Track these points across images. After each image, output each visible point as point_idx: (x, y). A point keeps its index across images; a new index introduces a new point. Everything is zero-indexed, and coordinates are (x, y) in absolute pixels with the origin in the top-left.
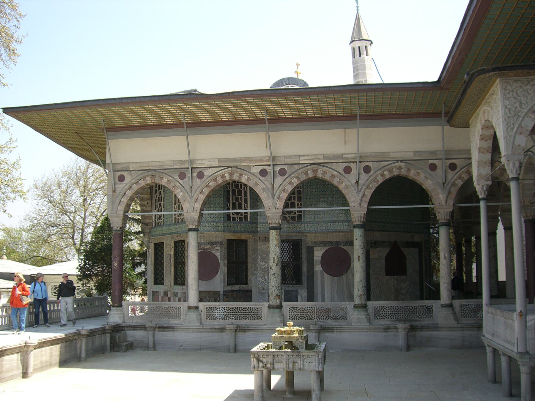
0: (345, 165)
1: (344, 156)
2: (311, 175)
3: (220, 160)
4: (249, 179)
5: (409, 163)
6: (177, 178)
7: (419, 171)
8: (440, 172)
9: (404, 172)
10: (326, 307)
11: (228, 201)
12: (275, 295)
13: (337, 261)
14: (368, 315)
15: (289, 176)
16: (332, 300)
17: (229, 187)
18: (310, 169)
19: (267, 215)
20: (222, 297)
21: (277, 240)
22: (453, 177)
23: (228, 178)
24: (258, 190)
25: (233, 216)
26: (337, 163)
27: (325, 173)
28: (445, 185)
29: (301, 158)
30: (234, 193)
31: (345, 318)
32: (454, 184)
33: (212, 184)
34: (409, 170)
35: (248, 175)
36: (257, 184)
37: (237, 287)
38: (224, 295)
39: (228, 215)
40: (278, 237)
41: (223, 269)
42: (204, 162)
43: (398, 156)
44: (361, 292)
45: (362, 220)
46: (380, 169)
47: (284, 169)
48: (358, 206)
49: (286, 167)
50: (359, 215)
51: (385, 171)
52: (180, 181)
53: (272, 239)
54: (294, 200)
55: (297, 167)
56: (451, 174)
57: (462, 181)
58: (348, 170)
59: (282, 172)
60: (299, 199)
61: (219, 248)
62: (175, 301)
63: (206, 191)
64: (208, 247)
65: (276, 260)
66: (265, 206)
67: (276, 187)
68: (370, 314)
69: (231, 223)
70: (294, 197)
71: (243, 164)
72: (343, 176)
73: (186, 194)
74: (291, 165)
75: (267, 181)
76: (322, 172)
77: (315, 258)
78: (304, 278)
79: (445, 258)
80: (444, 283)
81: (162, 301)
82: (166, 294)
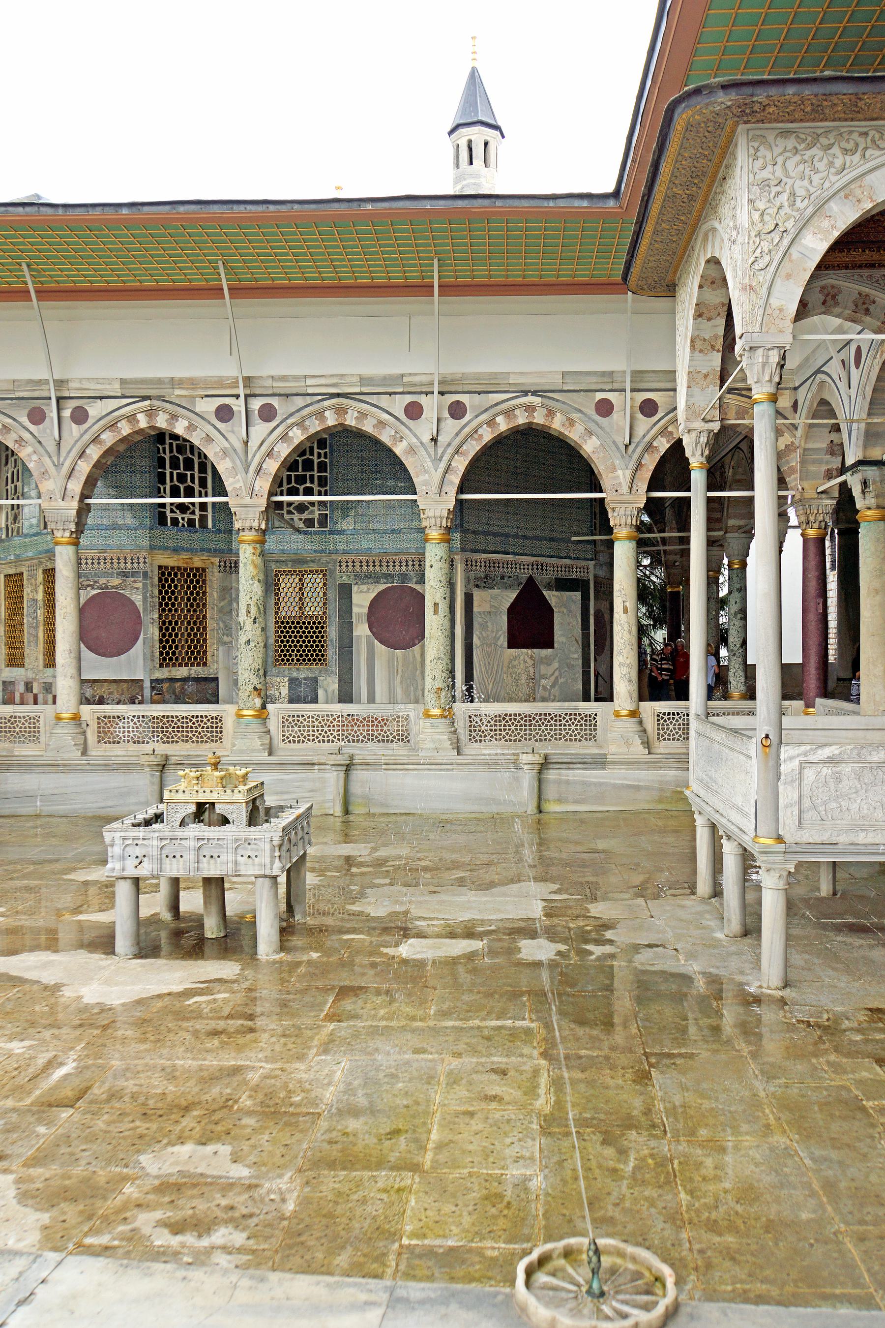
0: (409, 399)
1: (405, 380)
2: (331, 420)
3: (123, 381)
4: (191, 427)
5: (553, 399)
6: (25, 420)
7: (575, 416)
8: (620, 419)
9: (539, 418)
10: (379, 715)
11: (163, 482)
12: (251, 688)
13: (398, 617)
14: (455, 732)
15: (282, 422)
16: (392, 699)
17: (164, 449)
18: (329, 408)
19: (233, 510)
20: (147, 692)
21: (256, 566)
22: (648, 432)
23: (143, 422)
24: (211, 452)
25: (174, 515)
26: (390, 394)
27: (363, 415)
28: (631, 448)
29: (309, 382)
30: (175, 464)
31: (404, 738)
32: (649, 447)
33: (109, 439)
34: (550, 413)
35: (188, 419)
36: (209, 439)
37: (182, 672)
38: (153, 688)
39: (160, 516)
40: (259, 561)
41: (151, 632)
42: (86, 385)
43: (529, 381)
44: (439, 683)
45: (444, 524)
46: (486, 410)
47: (270, 406)
48: (435, 492)
49: (274, 401)
50: (437, 514)
51: (497, 415)
52: (32, 428)
53: (245, 564)
54: (312, 482)
55: (300, 402)
56: (644, 424)
57: (668, 442)
58: (414, 411)
59: (267, 413)
60: (323, 482)
61: (140, 585)
62: (46, 703)
63: (95, 453)
64: (115, 582)
65: (254, 610)
66: (229, 489)
67: (253, 444)
68: (459, 730)
69: (169, 531)
70: (312, 477)
71: (178, 392)
72: (402, 423)
73: (46, 460)
74: (287, 396)
75: (233, 432)
76: (356, 414)
77: (355, 610)
78: (332, 653)
79: (625, 611)
80: (621, 664)
81: (22, 703)
82: (28, 687)
